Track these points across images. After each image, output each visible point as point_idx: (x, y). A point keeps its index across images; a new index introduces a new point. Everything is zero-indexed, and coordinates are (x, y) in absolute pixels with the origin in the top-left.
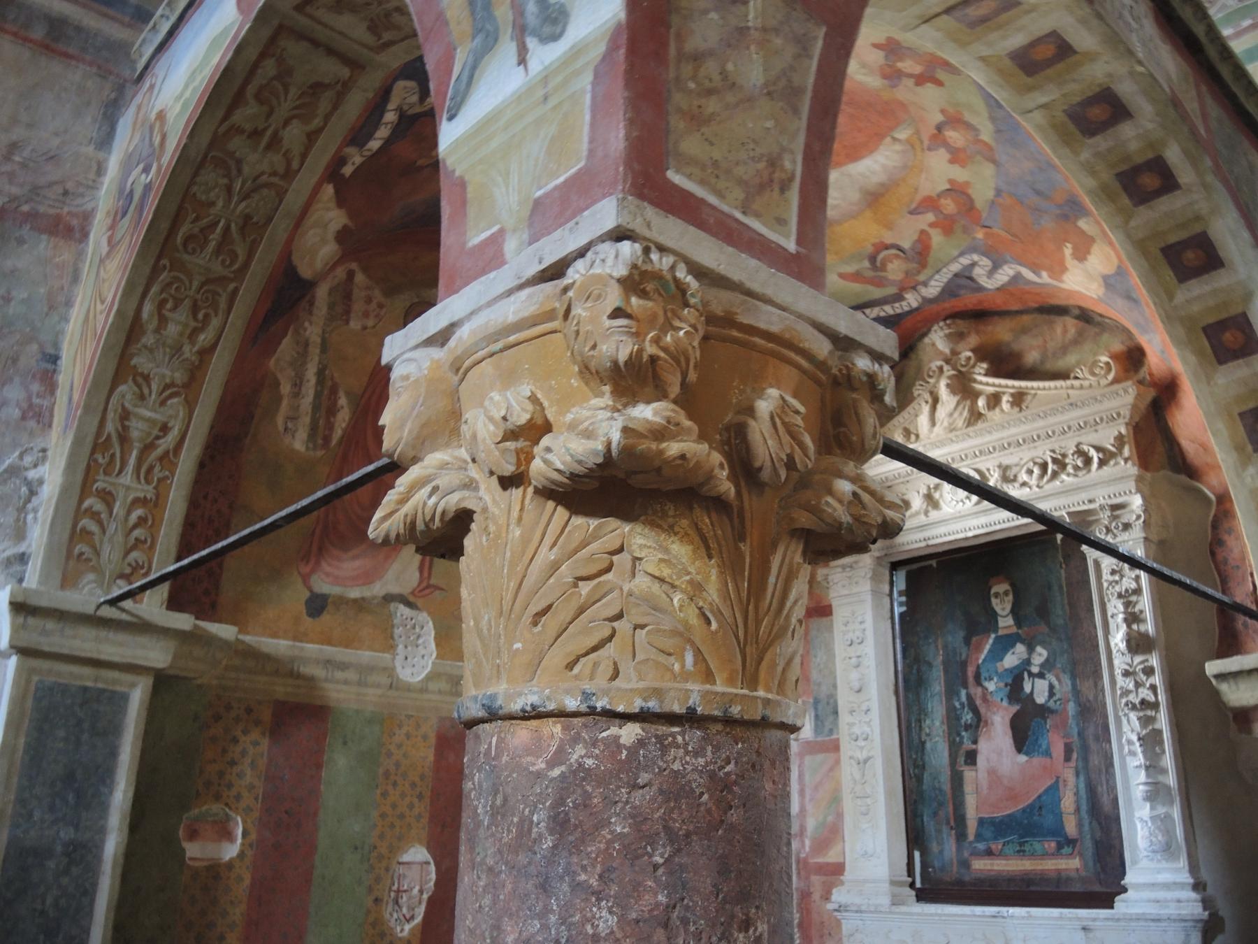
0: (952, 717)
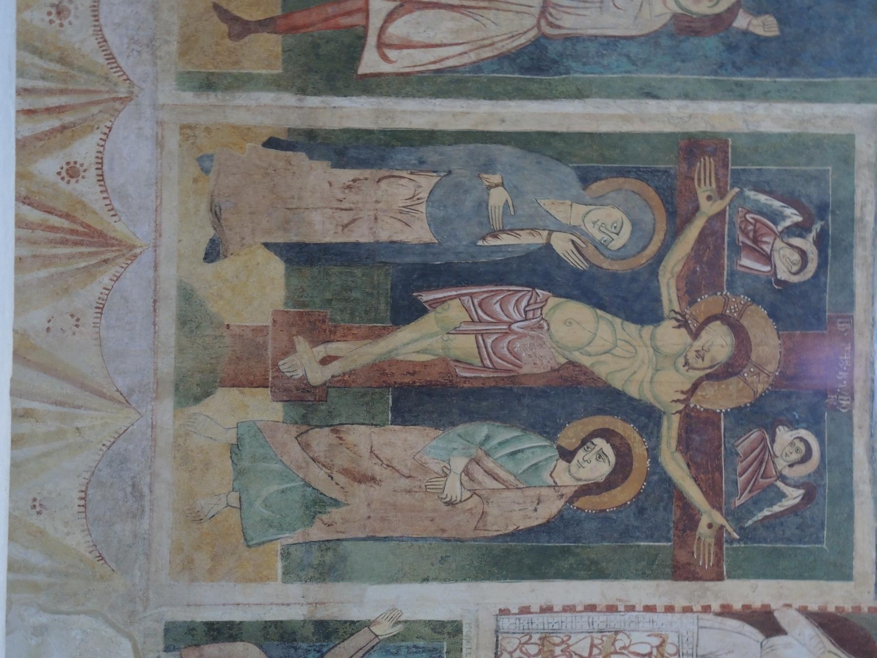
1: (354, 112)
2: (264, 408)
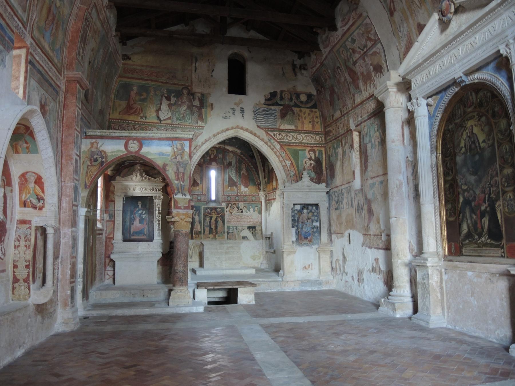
0: (130, 219)
2: (217, 235)
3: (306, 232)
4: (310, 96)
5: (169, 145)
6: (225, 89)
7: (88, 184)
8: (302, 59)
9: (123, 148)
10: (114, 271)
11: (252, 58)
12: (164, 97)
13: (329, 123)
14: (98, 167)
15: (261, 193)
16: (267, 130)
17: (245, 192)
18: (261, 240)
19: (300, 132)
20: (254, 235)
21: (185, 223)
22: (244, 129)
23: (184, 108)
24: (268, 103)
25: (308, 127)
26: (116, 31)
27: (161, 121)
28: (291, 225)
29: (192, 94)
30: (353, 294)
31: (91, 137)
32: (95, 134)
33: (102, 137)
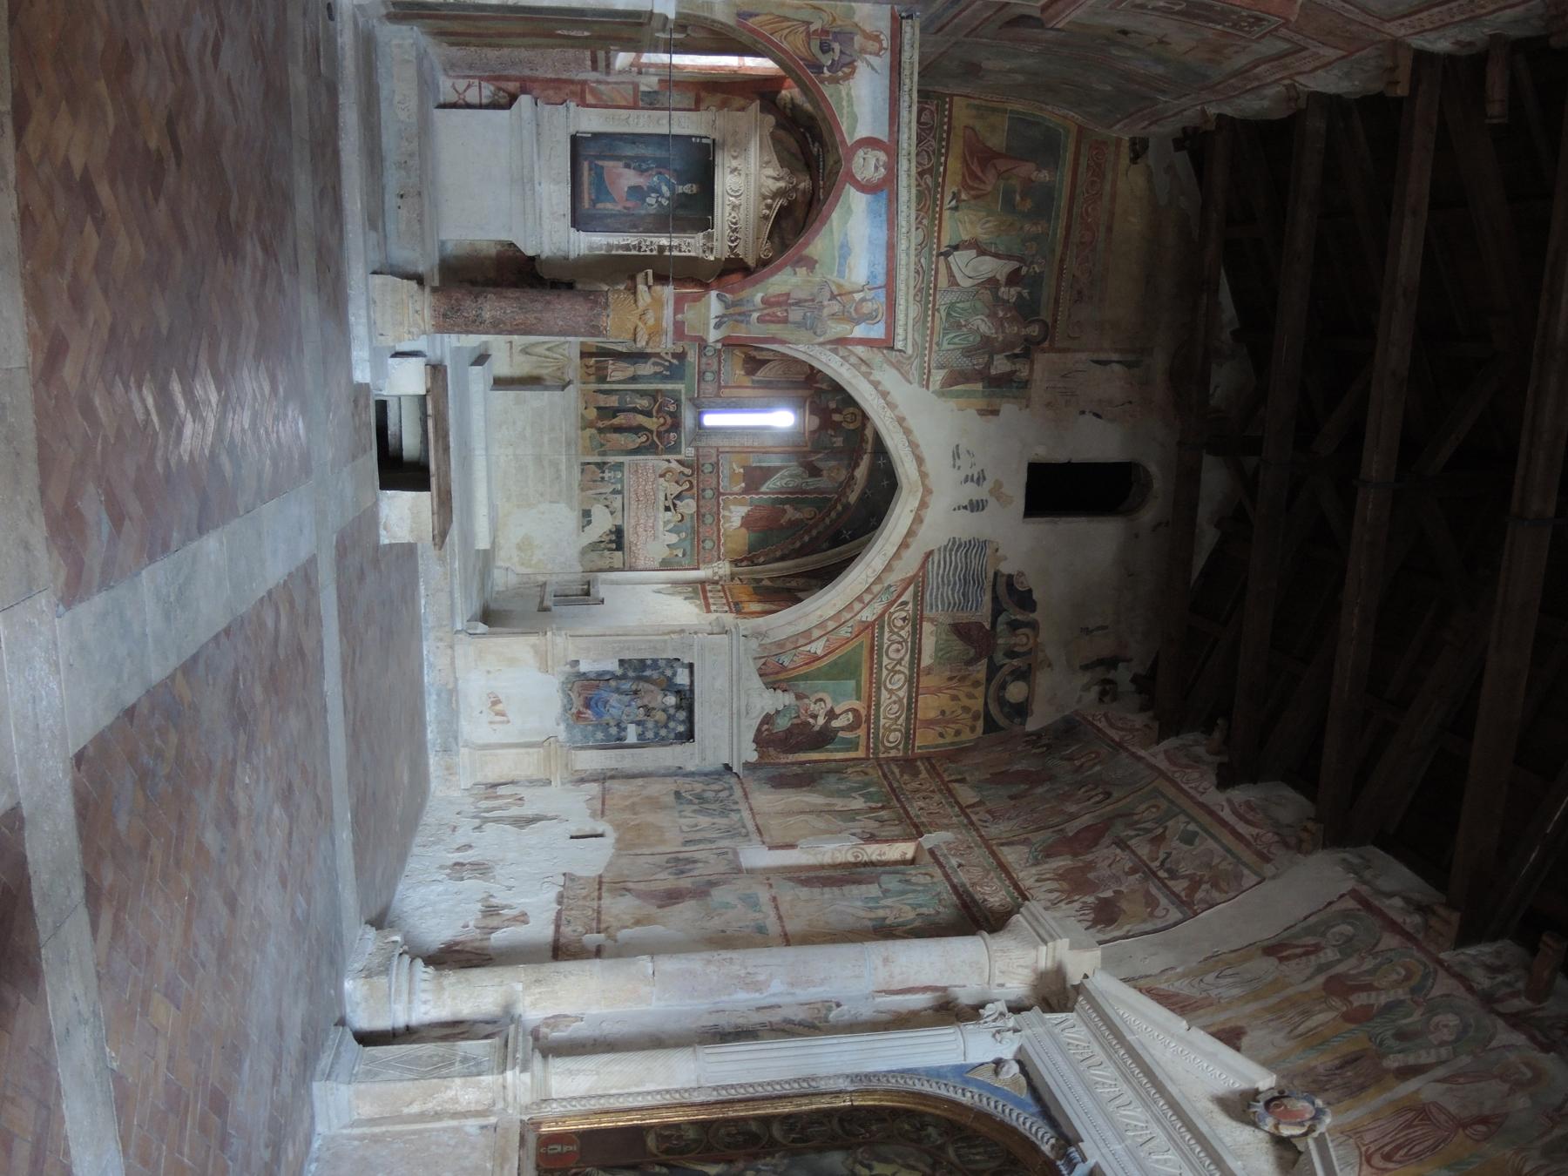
0: (642, 159)
1: (606, 387)
2: (594, 431)
3: (607, 702)
4: (1021, 710)
5: (873, 276)
6: (1042, 453)
7: (751, 22)
8: (1133, 688)
9: (862, 132)
10: (481, 106)
11: (1137, 536)
12: (1016, 265)
13: (940, 770)
14: (806, 54)
15: (724, 568)
16: (919, 582)
17: (728, 519)
18: (580, 569)
19: (913, 682)
20: (595, 546)
21: (630, 326)
22: (922, 513)
23: (983, 325)
24: (1002, 581)
25: (929, 706)
26: (1220, 116)
27: (946, 255)
28: (627, 656)
29: (1027, 351)
30: (415, 850)
31: (896, 33)
32: (907, 47)
33: (896, 68)
